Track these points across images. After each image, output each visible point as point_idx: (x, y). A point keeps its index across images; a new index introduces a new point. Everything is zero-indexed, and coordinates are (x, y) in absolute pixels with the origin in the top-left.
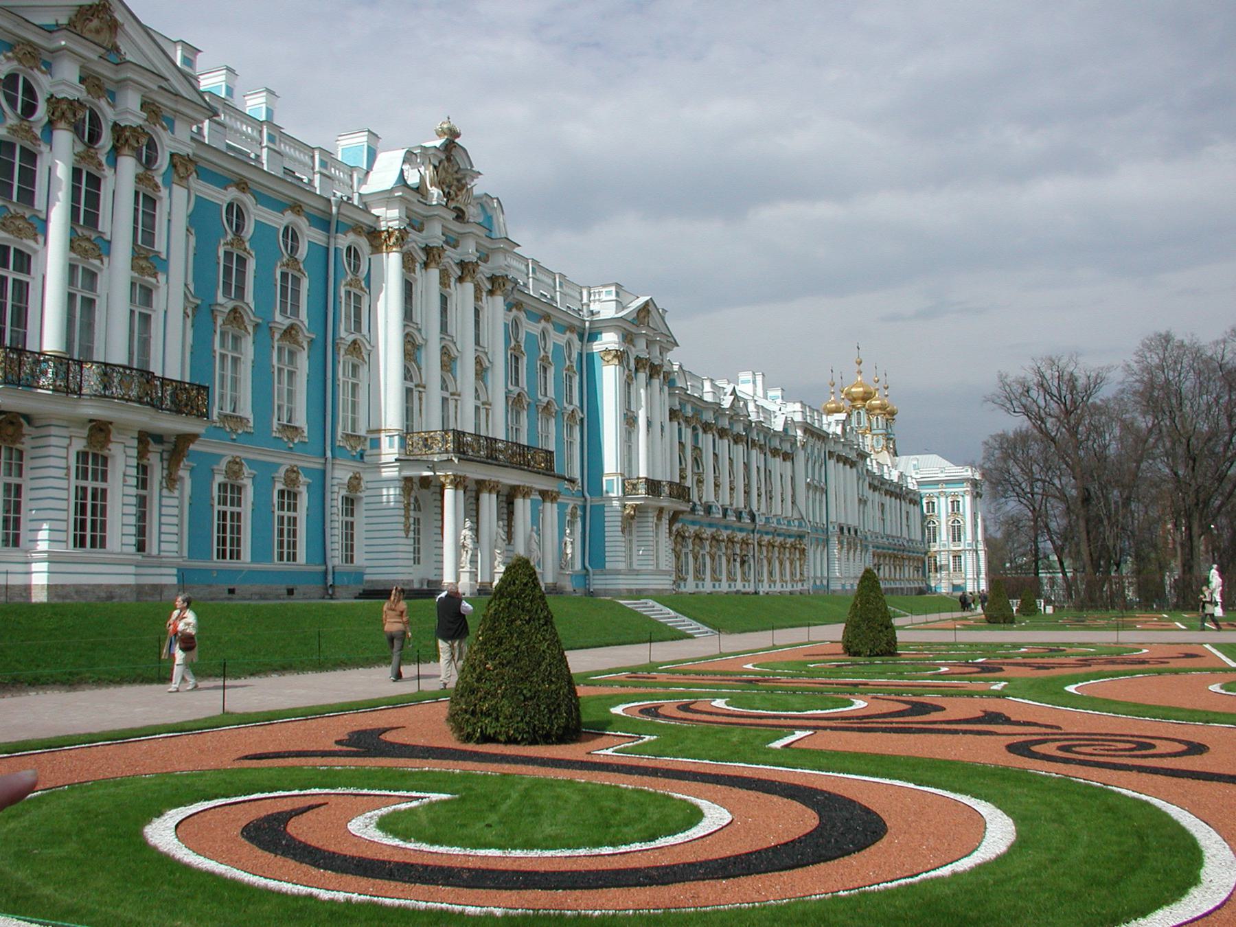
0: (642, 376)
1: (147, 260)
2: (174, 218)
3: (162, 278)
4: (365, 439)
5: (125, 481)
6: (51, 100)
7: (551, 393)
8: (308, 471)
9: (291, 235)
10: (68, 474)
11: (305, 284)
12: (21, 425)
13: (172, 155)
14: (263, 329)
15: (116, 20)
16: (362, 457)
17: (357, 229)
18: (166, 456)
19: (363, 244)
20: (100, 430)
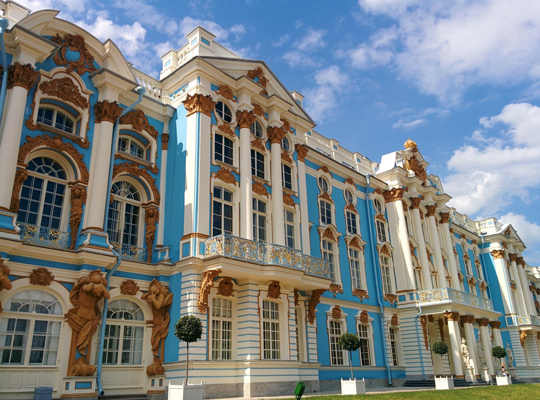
0: (514, 263)
1: (290, 199)
2: (299, 176)
3: (297, 206)
4: (396, 296)
5: (289, 316)
6: (238, 113)
7: (471, 273)
8: (372, 314)
9: (349, 194)
10: (259, 312)
11: (358, 218)
12: (232, 285)
13: (296, 146)
14: (342, 240)
15: (265, 79)
16: (395, 306)
17: (378, 191)
18: (307, 303)
19: (381, 198)
20: (274, 288)
